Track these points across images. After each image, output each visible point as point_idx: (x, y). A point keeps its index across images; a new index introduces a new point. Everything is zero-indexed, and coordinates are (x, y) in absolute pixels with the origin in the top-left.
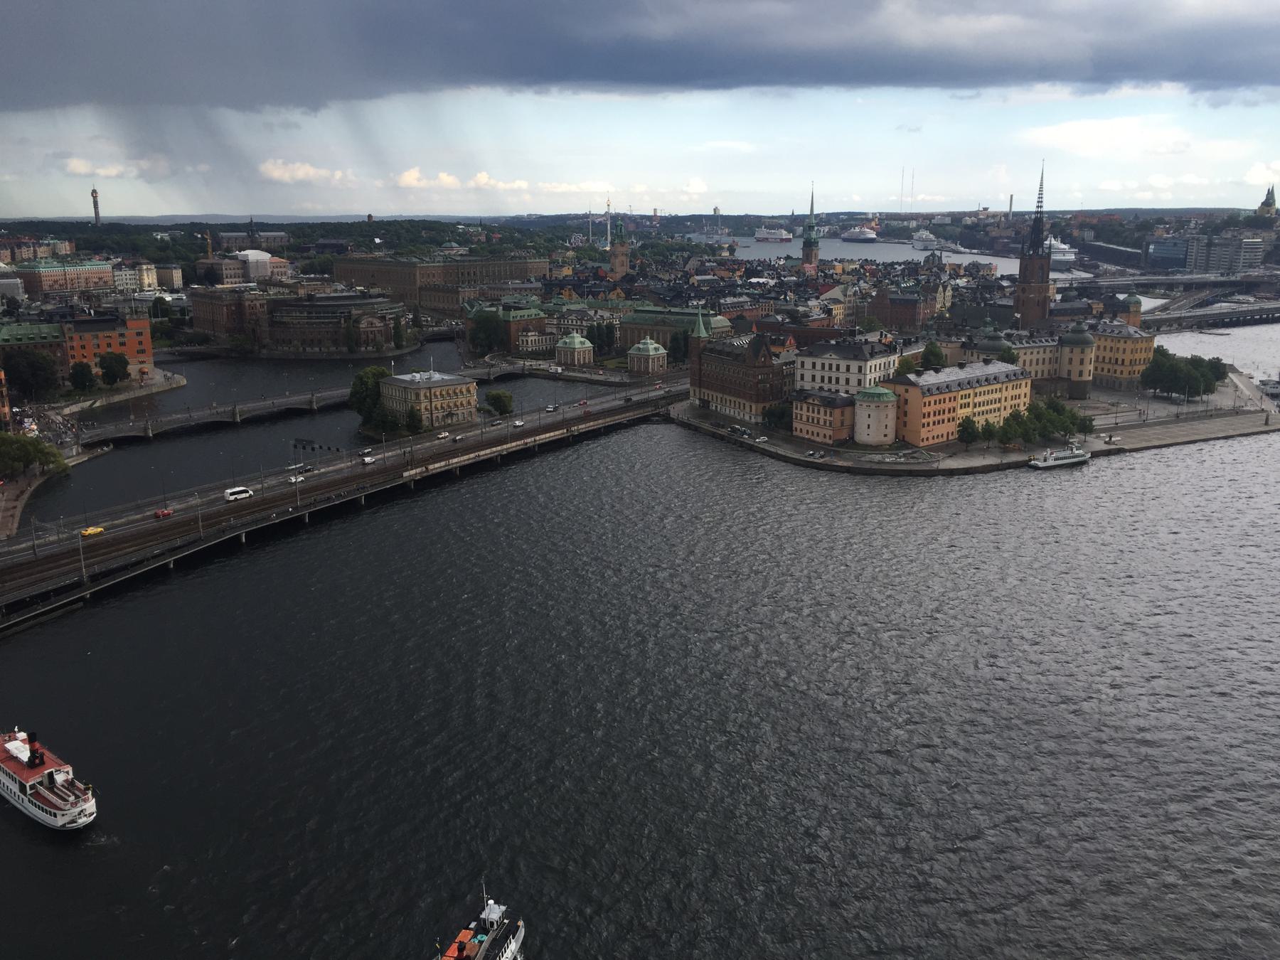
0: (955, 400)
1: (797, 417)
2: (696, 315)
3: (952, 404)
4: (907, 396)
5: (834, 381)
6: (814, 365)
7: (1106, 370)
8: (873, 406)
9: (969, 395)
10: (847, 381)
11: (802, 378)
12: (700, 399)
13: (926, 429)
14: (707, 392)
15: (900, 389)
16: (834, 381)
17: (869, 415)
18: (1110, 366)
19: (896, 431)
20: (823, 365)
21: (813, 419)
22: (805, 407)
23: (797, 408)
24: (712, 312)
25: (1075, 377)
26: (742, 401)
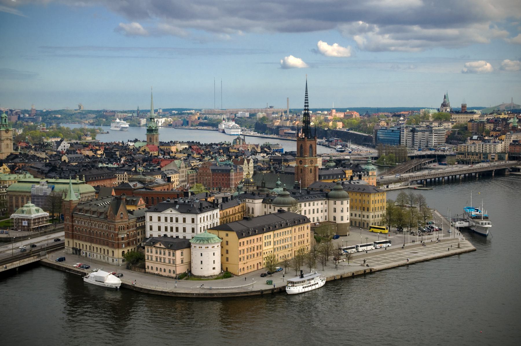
0: (260, 240)
1: (148, 258)
3: (259, 244)
4: (226, 239)
5: (174, 229)
7: (358, 215)
8: (204, 247)
9: (270, 235)
10: (184, 230)
11: (151, 229)
12: (73, 248)
14: (78, 242)
15: (223, 234)
16: (174, 229)
17: (201, 254)
21: (160, 259)
23: (148, 251)
25: (339, 221)
26: (106, 248)
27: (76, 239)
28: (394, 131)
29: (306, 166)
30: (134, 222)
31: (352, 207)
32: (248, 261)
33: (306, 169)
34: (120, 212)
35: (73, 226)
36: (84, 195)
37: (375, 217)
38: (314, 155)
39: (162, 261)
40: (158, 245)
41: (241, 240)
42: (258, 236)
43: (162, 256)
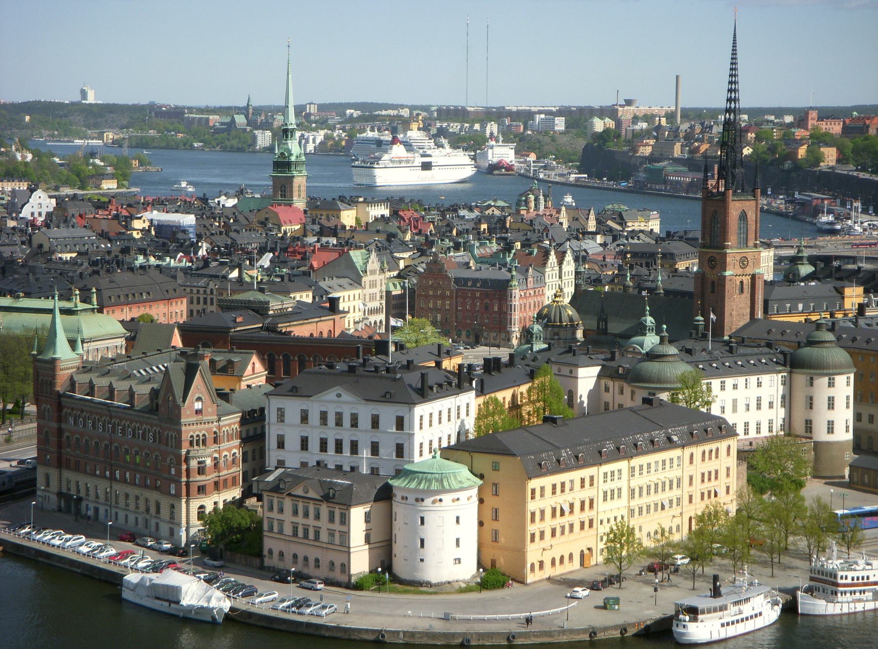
0: (592, 484)
1: (271, 529)
2: (51, 311)
3: (587, 493)
6: (304, 418)
9: (620, 471)
11: (281, 445)
12: (60, 494)
13: (538, 544)
15: (484, 461)
20: (324, 416)
22: (288, 503)
24: (81, 306)
25: (821, 435)
27: (68, 468)
29: (728, 273)
30: (234, 423)
31: (861, 396)
32: (554, 541)
33: (727, 282)
34: (193, 395)
35: (60, 432)
36: (93, 345)
38: (751, 243)
39: (311, 536)
41: (535, 483)
42: (586, 473)
43: (311, 522)
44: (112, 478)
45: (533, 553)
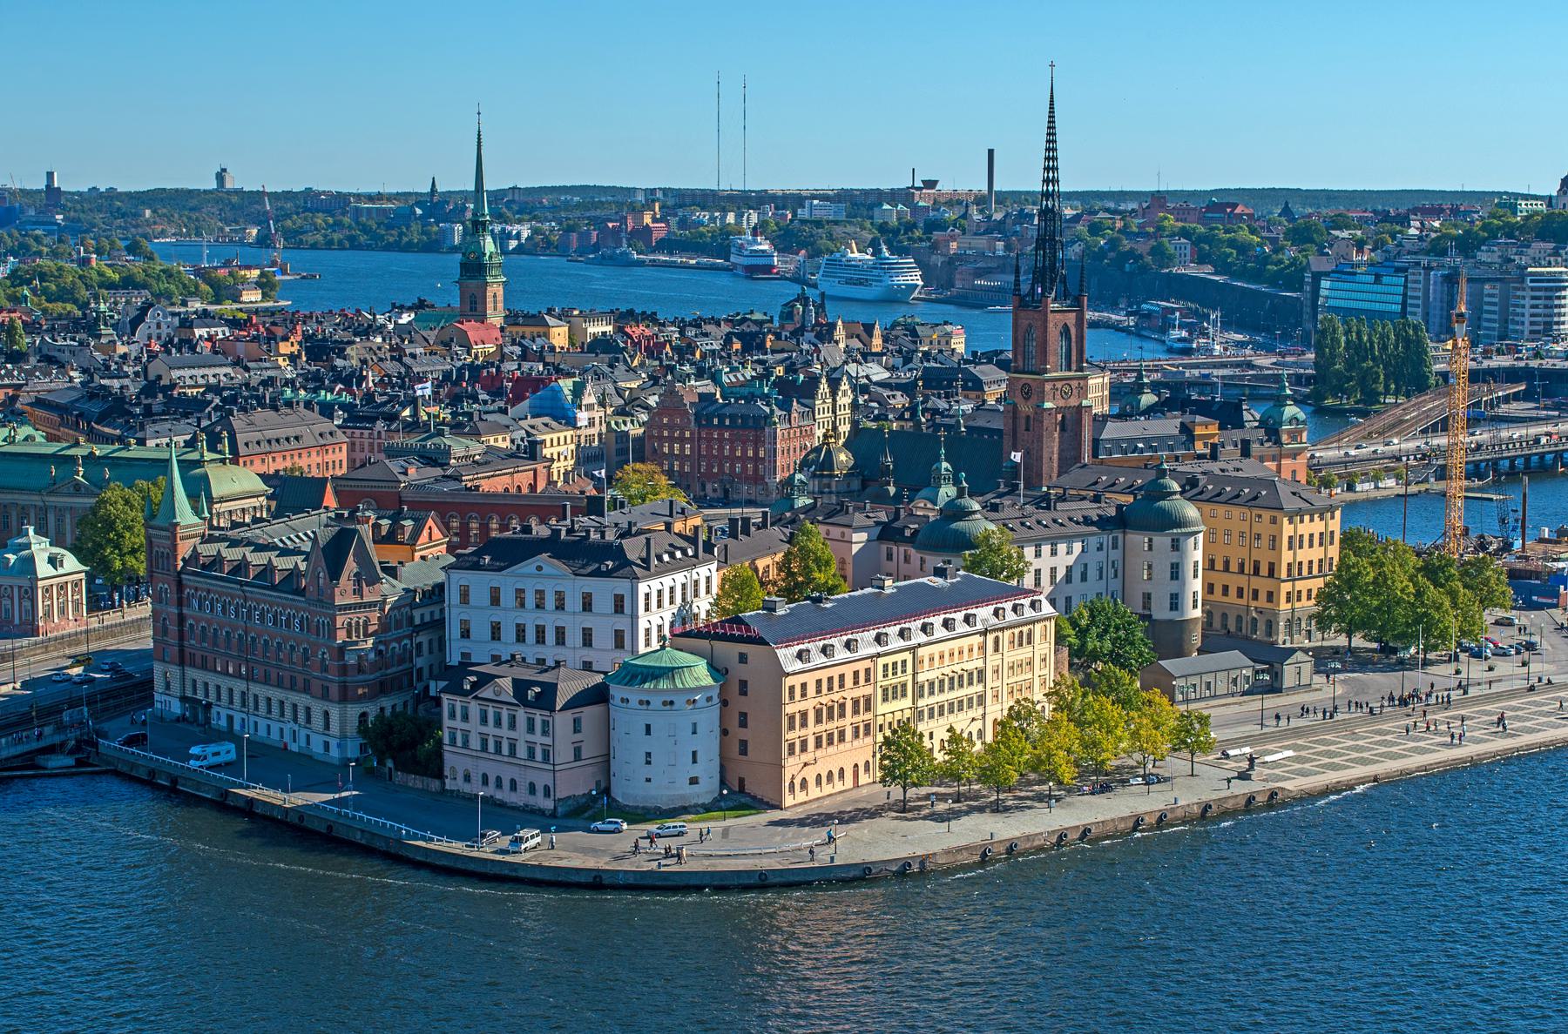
1: (453, 742)
4: (740, 671)
5: (550, 637)
7: (1233, 591)
9: (904, 662)
10: (587, 640)
11: (466, 634)
12: (183, 699)
15: (728, 651)
16: (550, 637)
17: (648, 728)
18: (1242, 581)
19: (722, 766)
20: (520, 592)
21: (498, 745)
23: (452, 716)
24: (208, 456)
26: (302, 700)
27: (193, 665)
28: (1385, 280)
30: (404, 606)
32: (819, 753)
35: (181, 619)
36: (225, 507)
37: (1299, 599)
39: (505, 750)
40: (487, 692)
44: (249, 678)
45: (792, 766)
